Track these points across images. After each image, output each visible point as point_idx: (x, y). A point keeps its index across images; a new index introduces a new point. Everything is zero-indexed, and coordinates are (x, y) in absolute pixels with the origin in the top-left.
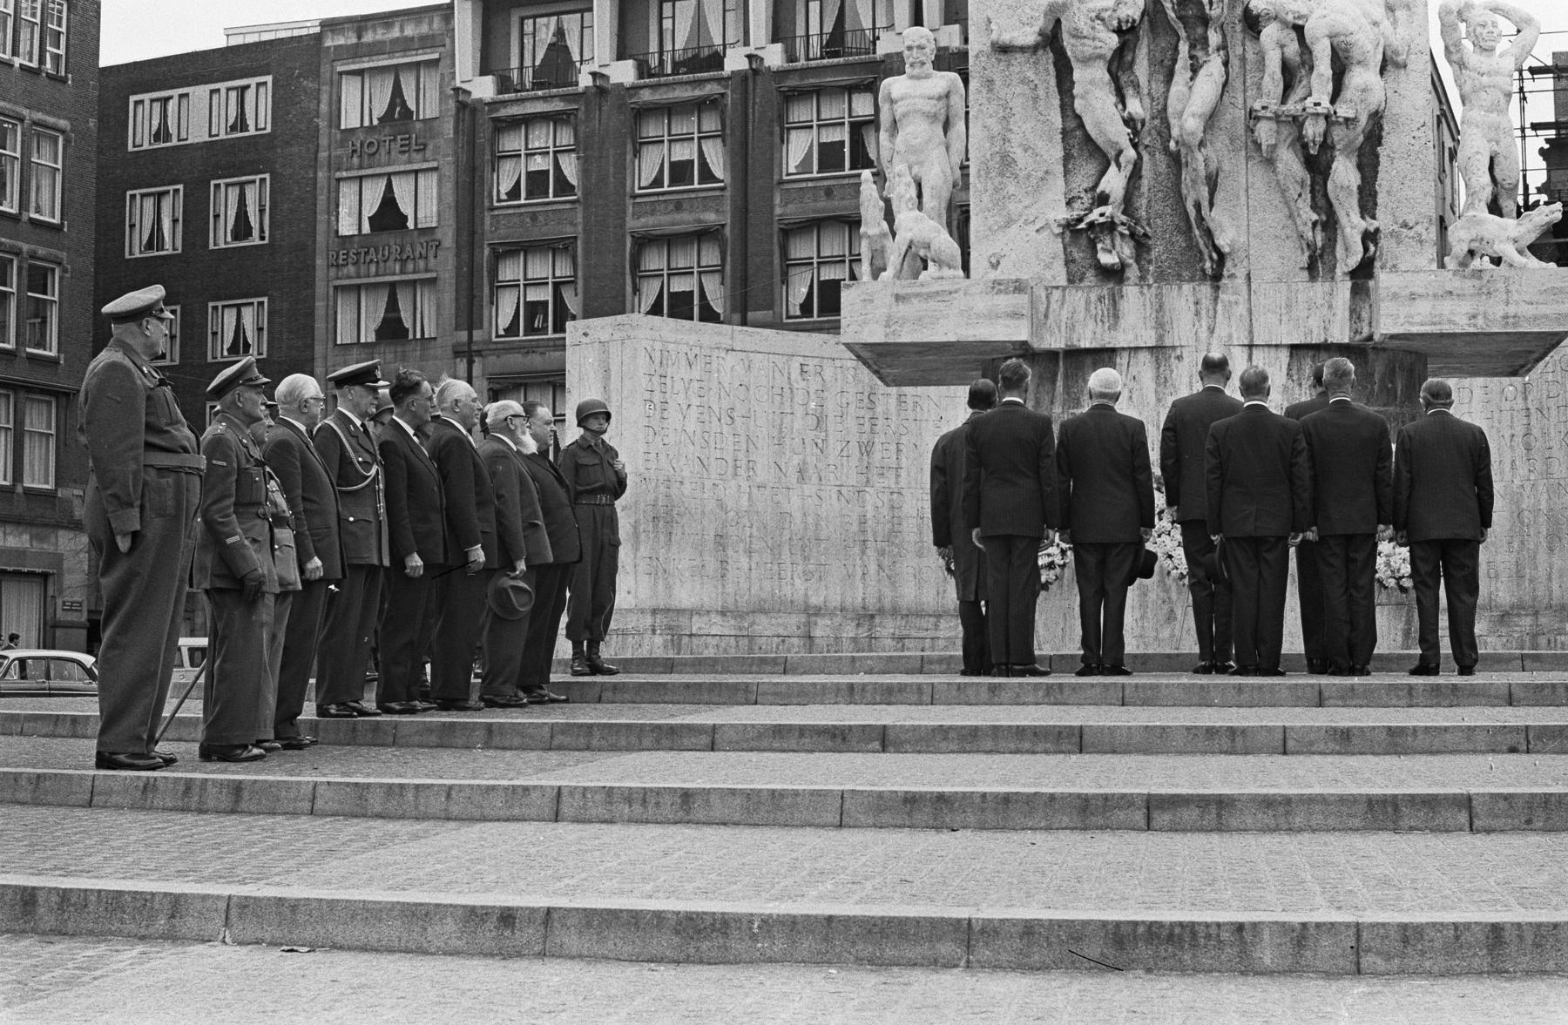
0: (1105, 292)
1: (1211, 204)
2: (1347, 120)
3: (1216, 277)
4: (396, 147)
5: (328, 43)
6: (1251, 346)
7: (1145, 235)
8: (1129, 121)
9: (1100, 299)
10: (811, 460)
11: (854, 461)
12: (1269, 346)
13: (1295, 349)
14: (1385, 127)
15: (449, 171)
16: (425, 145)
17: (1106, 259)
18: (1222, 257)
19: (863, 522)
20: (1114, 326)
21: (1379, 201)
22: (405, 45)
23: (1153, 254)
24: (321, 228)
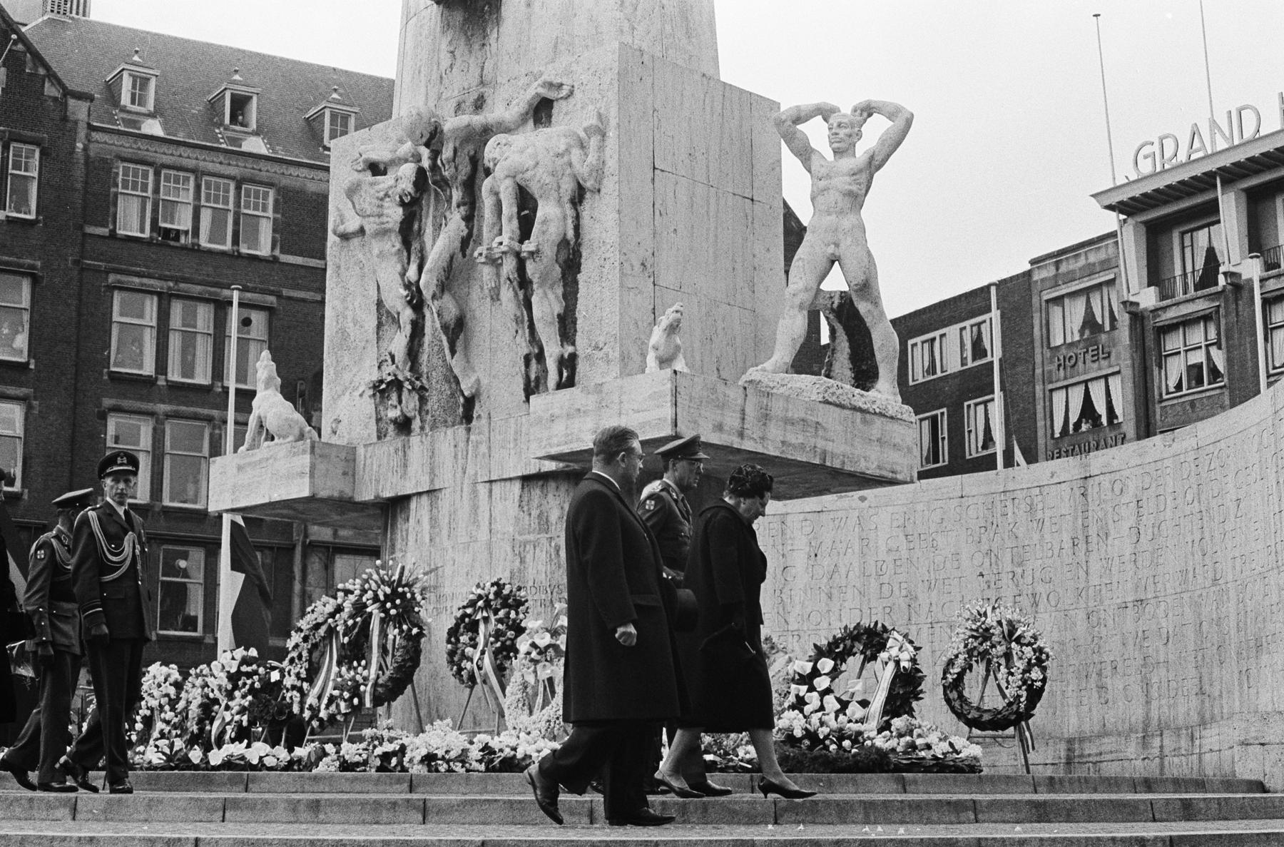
0: (400, 445)
1: (453, 352)
2: (532, 253)
3: (468, 417)
4: (1088, 357)
5: (1036, 277)
6: (491, 482)
7: (423, 388)
8: (408, 286)
9: (396, 451)
12: (505, 480)
13: (527, 480)
14: (584, 254)
15: (1127, 372)
16: (1109, 354)
17: (393, 414)
18: (470, 403)
20: (404, 475)
21: (578, 327)
22: (1090, 271)
23: (429, 407)
24: (1040, 433)
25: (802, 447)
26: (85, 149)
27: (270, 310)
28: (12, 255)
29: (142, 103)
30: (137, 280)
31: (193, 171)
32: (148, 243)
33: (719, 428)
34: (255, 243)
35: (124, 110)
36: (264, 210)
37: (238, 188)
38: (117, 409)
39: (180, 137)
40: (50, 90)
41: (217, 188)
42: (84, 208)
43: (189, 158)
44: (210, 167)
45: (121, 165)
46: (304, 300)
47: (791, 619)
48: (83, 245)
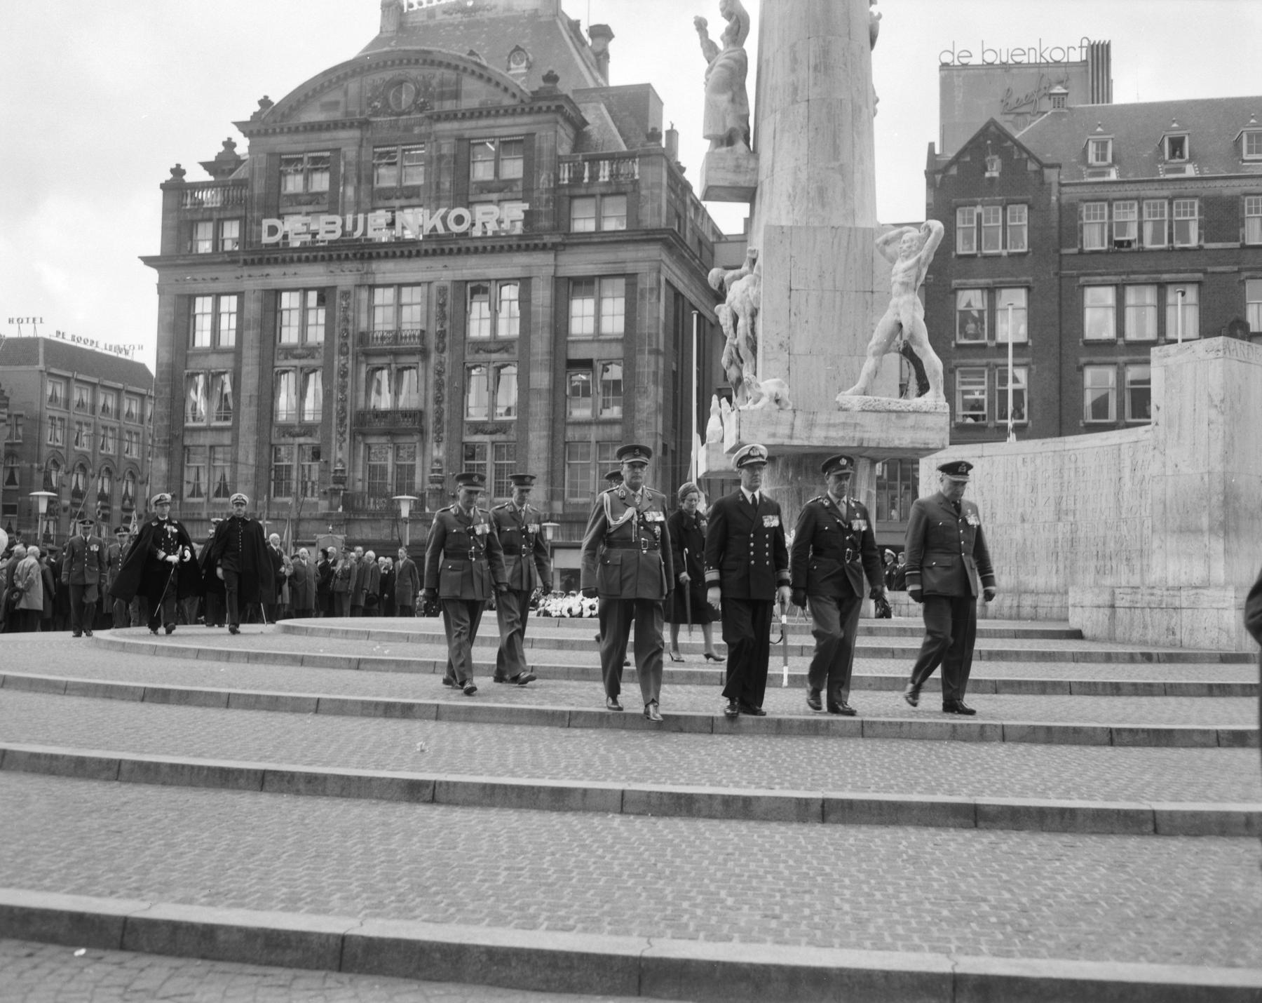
10: (1029, 510)
11: (1053, 508)
19: (1056, 542)
25: (843, 438)
26: (1058, 200)
27: (1199, 283)
28: (1012, 275)
29: (1104, 158)
30: (1099, 278)
31: (1137, 198)
32: (1107, 252)
33: (774, 435)
34: (1188, 241)
35: (1089, 166)
36: (1192, 214)
37: (1170, 204)
38: (1091, 364)
39: (1131, 177)
40: (1032, 166)
41: (1155, 207)
42: (1060, 238)
43: (1131, 191)
44: (1149, 193)
45: (1084, 207)
46: (1224, 273)
47: (1123, 511)
48: (1060, 262)
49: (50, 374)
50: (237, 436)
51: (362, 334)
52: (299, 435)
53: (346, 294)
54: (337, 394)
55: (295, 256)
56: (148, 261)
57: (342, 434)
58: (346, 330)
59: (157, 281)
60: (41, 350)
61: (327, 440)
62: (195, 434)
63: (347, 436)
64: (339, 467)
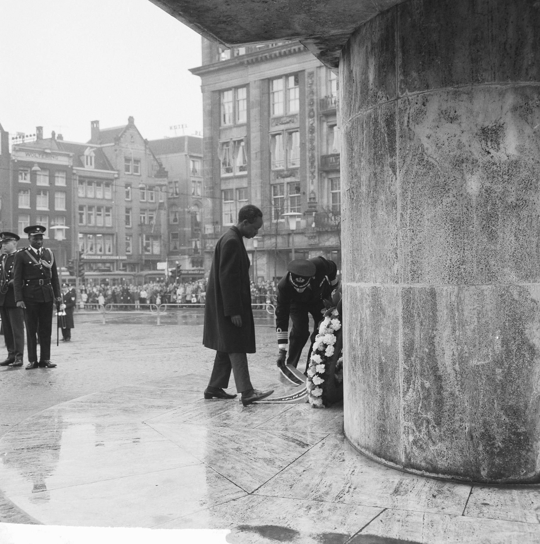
49: (191, 156)
50: (250, 179)
51: (323, 100)
52: (287, 176)
53: (311, 74)
54: (308, 145)
55: (277, 52)
56: (195, 71)
57: (312, 173)
58: (312, 100)
59: (201, 84)
60: (186, 143)
61: (304, 178)
62: (227, 181)
63: (316, 174)
64: (312, 196)
